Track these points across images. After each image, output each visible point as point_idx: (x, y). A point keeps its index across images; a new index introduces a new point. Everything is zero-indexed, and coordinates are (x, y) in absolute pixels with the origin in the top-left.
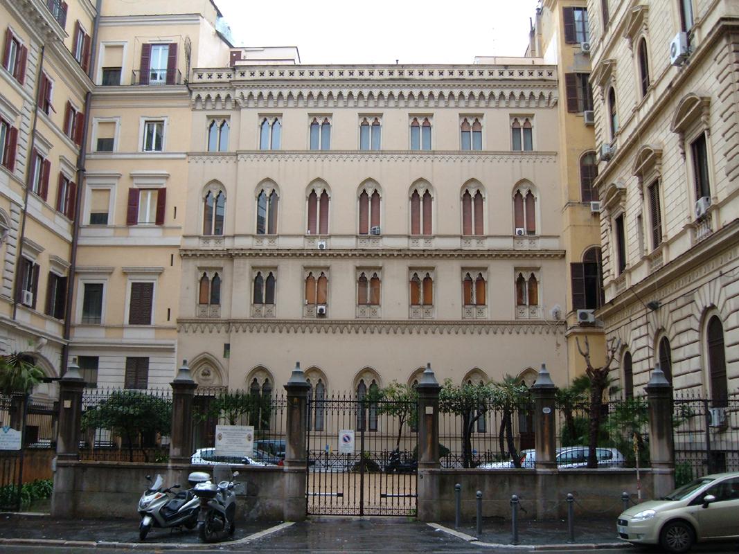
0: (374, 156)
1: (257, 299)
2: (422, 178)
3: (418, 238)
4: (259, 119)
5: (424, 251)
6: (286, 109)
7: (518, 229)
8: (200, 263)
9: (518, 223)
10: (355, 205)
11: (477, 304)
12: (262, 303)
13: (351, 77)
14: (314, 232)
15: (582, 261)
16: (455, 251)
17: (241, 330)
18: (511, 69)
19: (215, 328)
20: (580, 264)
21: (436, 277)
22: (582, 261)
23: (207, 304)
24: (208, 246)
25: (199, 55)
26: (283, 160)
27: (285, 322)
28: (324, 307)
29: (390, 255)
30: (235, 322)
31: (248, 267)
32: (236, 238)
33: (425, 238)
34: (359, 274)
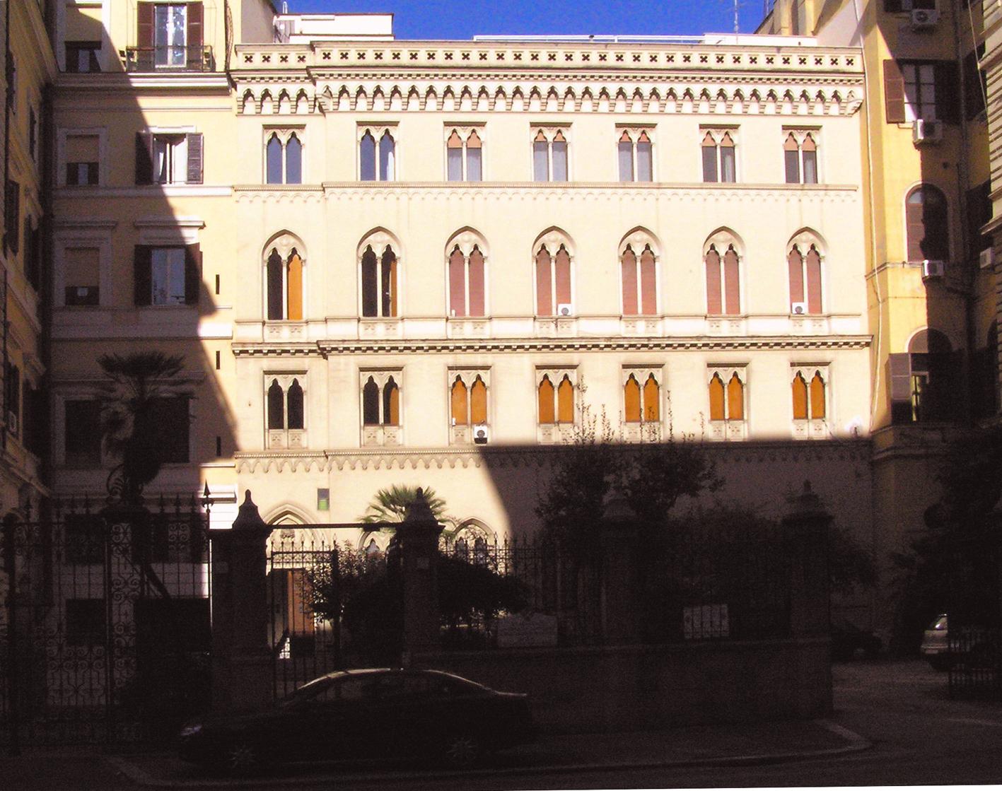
0: (560, 191)
1: (370, 417)
2: (725, 227)
3: (635, 320)
4: (783, 133)
5: (649, 339)
6: (579, 117)
7: (795, 305)
8: (450, 359)
9: (796, 293)
10: (530, 269)
11: (730, 419)
12: (724, 419)
13: (834, 67)
14: (460, 312)
15: (906, 351)
16: (698, 338)
17: (347, 466)
18: (785, 54)
19: (459, 460)
20: (906, 354)
21: (665, 378)
22: (906, 351)
23: (466, 424)
24: (300, 338)
25: (993, 35)
26: (404, 198)
27: (421, 453)
28: (484, 428)
29: (591, 345)
30: (337, 454)
31: (353, 370)
32: (329, 323)
33: (647, 320)
34: (540, 378)
